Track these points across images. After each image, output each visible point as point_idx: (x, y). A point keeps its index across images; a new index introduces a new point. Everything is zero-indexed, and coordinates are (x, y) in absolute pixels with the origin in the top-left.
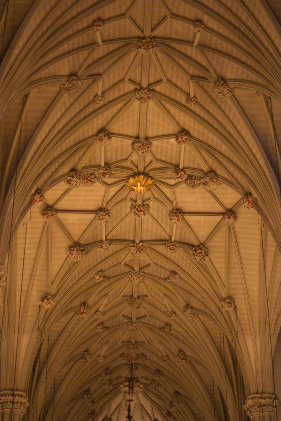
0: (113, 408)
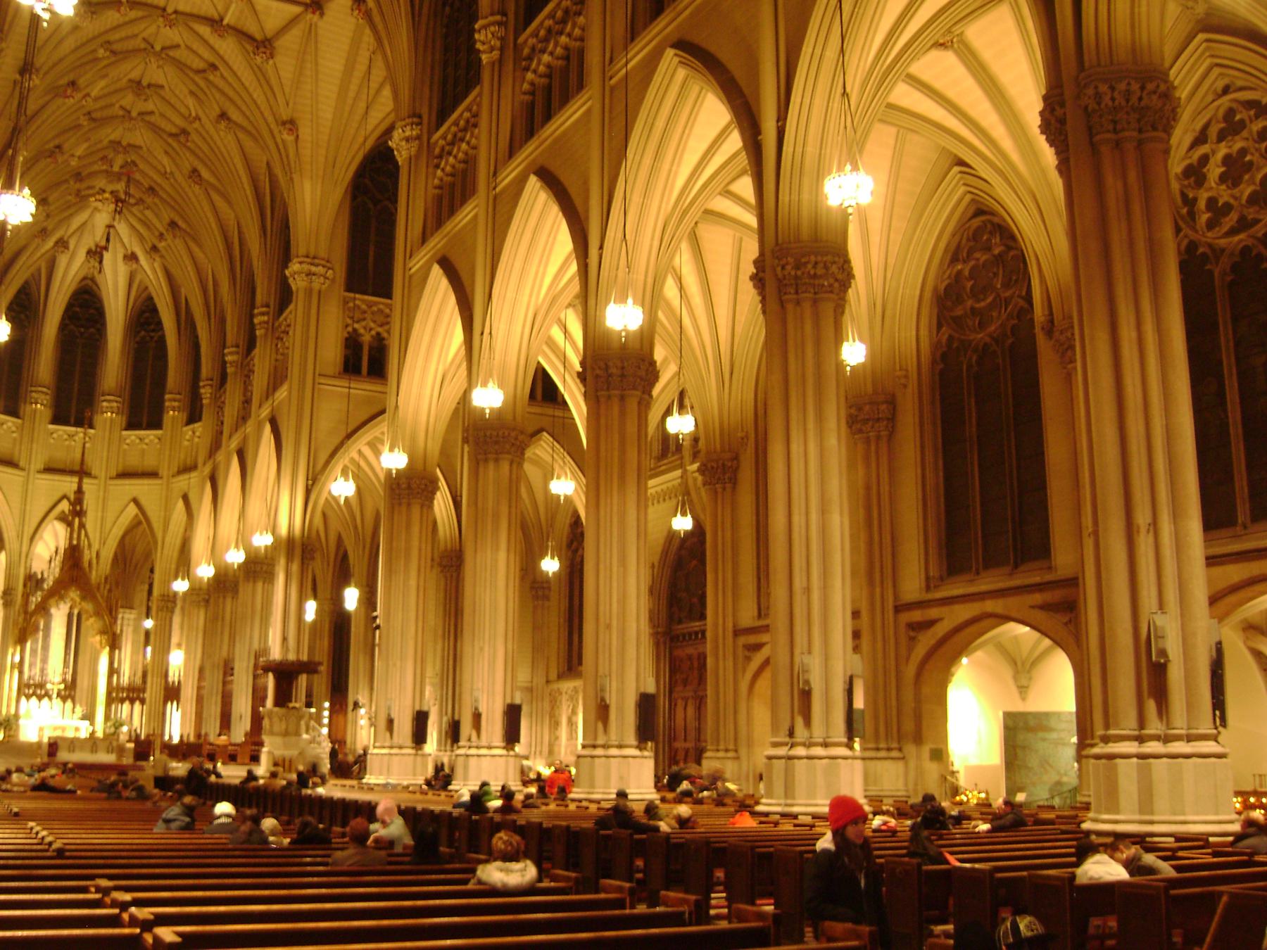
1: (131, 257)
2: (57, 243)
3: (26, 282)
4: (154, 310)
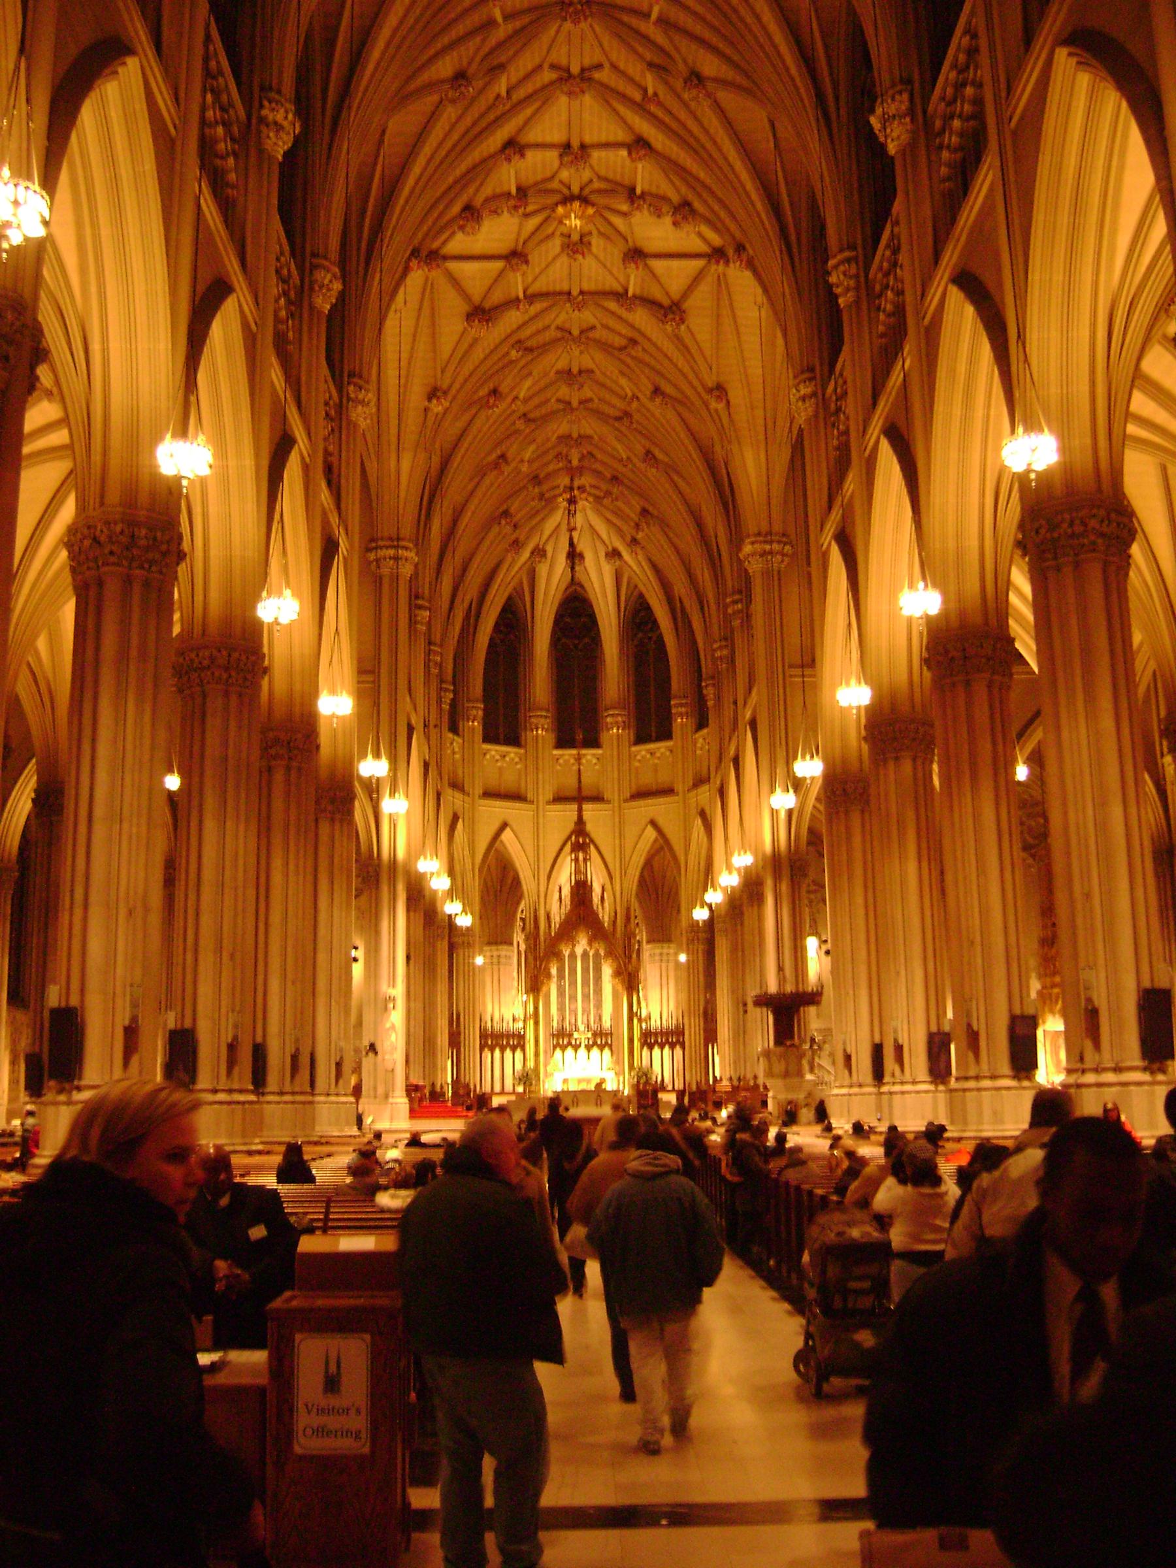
0: (547, 533)
1: (614, 554)
2: (532, 553)
3: (510, 598)
4: (648, 608)
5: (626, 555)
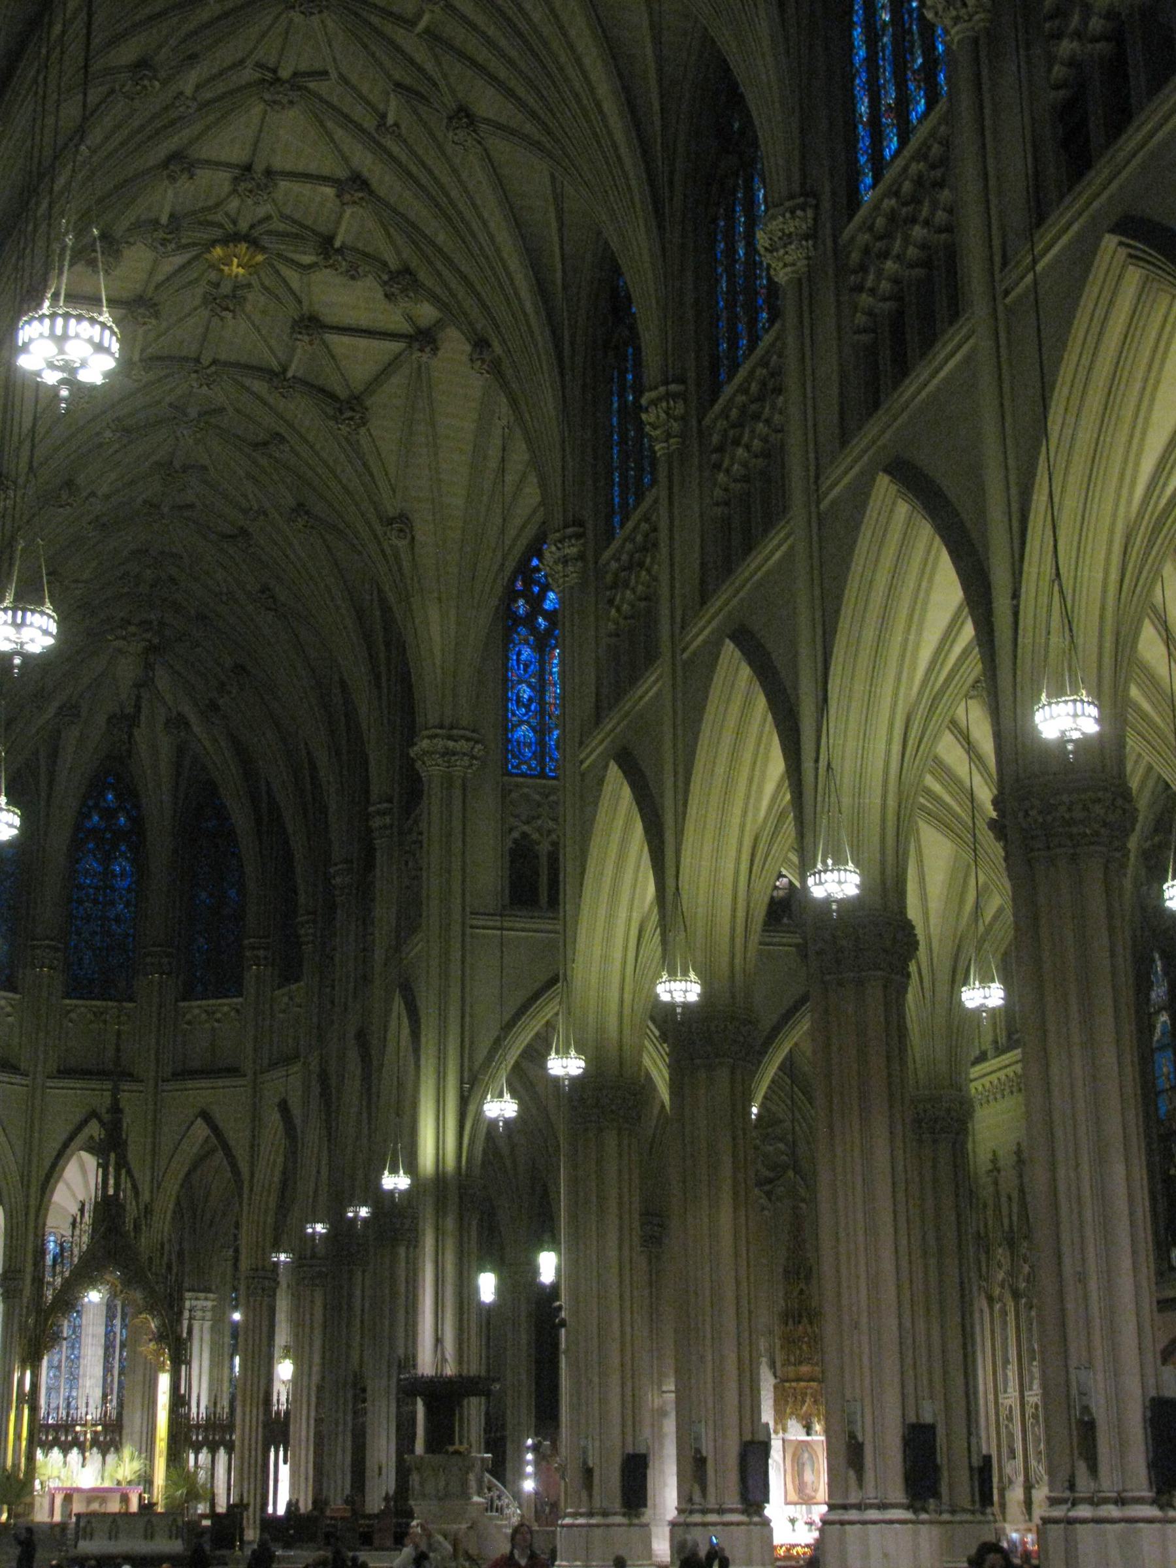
1: (178, 722)
2: (60, 708)
5: (197, 729)
